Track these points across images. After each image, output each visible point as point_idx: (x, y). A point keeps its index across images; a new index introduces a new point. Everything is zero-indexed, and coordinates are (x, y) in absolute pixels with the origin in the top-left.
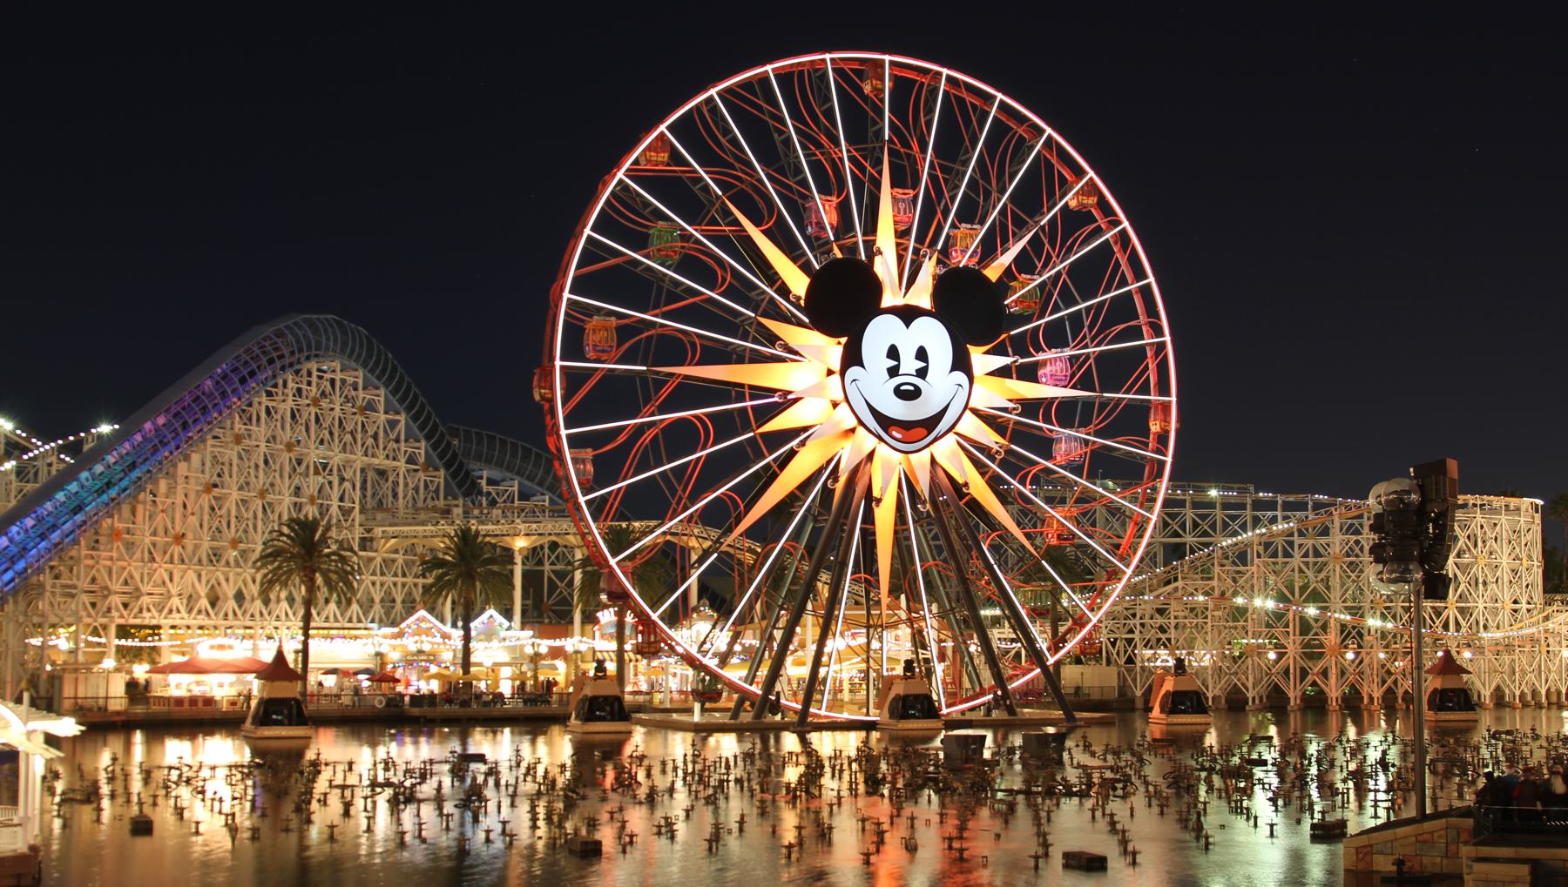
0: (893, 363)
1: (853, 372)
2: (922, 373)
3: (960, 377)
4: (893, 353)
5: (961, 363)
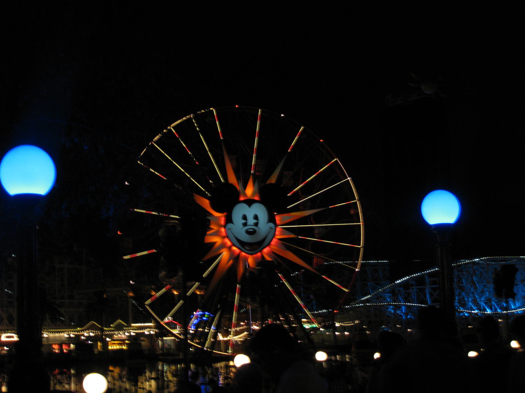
0: (244, 221)
1: (230, 225)
2: (256, 224)
3: (271, 225)
4: (245, 217)
5: (272, 219)
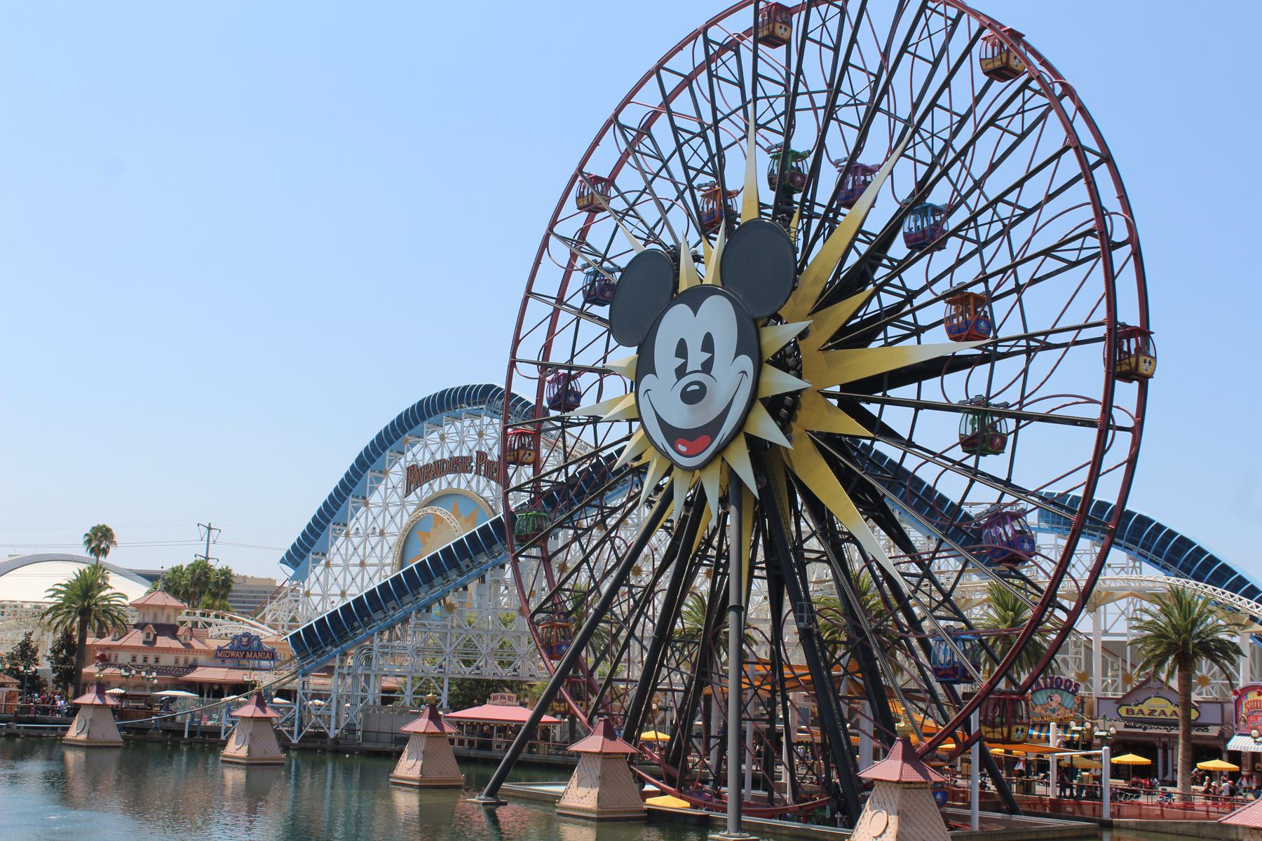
1: (648, 381)
2: (707, 367)
4: (682, 350)
5: (749, 343)
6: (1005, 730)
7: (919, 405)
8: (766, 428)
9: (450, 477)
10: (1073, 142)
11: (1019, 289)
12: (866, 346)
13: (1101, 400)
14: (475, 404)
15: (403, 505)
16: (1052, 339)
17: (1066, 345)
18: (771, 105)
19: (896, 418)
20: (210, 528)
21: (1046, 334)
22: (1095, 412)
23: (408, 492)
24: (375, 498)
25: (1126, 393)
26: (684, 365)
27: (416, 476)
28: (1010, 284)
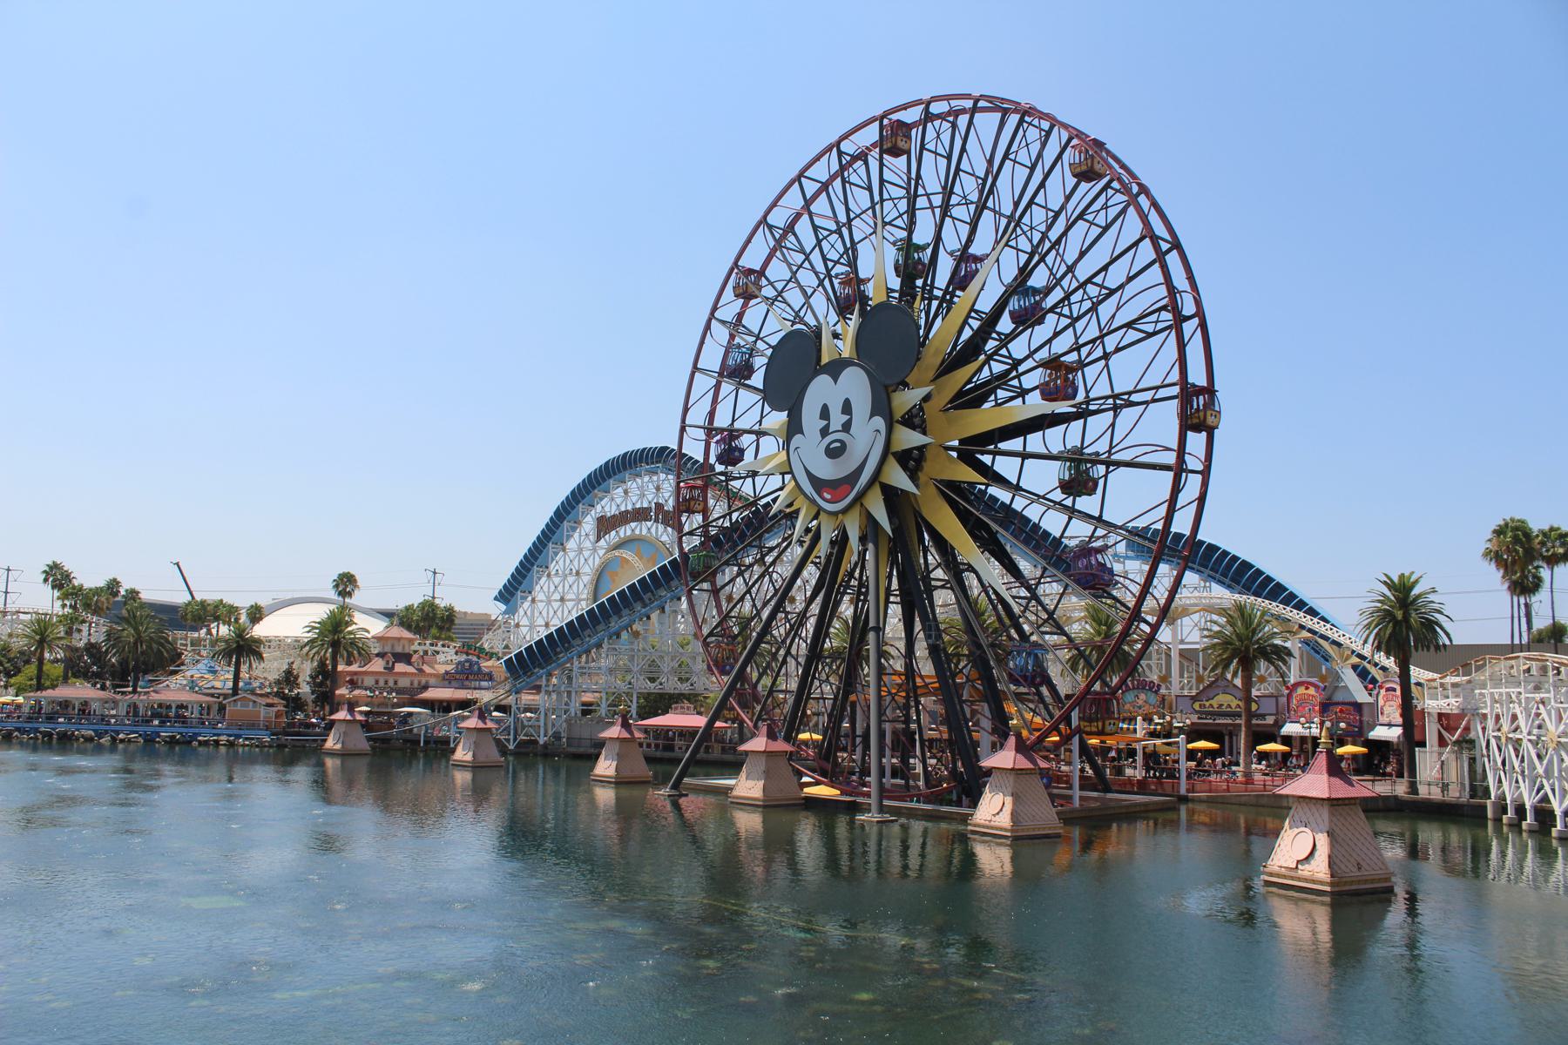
0: (825, 423)
1: (797, 440)
2: (847, 427)
4: (825, 413)
5: (881, 406)
6: (1100, 724)
7: (1024, 456)
8: (898, 478)
9: (633, 525)
10: (1149, 233)
11: (1106, 356)
12: (980, 406)
13: (1176, 448)
14: (653, 463)
15: (595, 550)
16: (1134, 398)
17: (1146, 403)
18: (895, 205)
19: (1006, 466)
20: (435, 573)
21: (1130, 393)
22: (1170, 458)
23: (599, 539)
24: (571, 545)
25: (1196, 441)
26: (828, 426)
27: (605, 525)
28: (1099, 353)
